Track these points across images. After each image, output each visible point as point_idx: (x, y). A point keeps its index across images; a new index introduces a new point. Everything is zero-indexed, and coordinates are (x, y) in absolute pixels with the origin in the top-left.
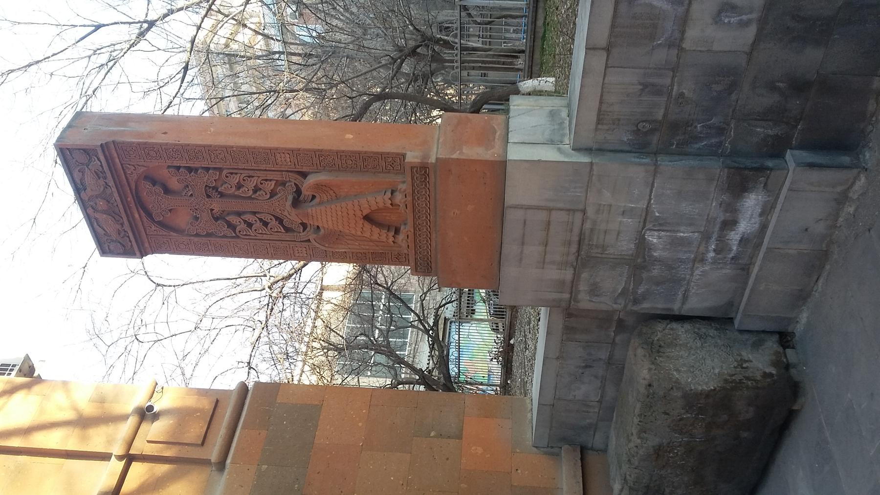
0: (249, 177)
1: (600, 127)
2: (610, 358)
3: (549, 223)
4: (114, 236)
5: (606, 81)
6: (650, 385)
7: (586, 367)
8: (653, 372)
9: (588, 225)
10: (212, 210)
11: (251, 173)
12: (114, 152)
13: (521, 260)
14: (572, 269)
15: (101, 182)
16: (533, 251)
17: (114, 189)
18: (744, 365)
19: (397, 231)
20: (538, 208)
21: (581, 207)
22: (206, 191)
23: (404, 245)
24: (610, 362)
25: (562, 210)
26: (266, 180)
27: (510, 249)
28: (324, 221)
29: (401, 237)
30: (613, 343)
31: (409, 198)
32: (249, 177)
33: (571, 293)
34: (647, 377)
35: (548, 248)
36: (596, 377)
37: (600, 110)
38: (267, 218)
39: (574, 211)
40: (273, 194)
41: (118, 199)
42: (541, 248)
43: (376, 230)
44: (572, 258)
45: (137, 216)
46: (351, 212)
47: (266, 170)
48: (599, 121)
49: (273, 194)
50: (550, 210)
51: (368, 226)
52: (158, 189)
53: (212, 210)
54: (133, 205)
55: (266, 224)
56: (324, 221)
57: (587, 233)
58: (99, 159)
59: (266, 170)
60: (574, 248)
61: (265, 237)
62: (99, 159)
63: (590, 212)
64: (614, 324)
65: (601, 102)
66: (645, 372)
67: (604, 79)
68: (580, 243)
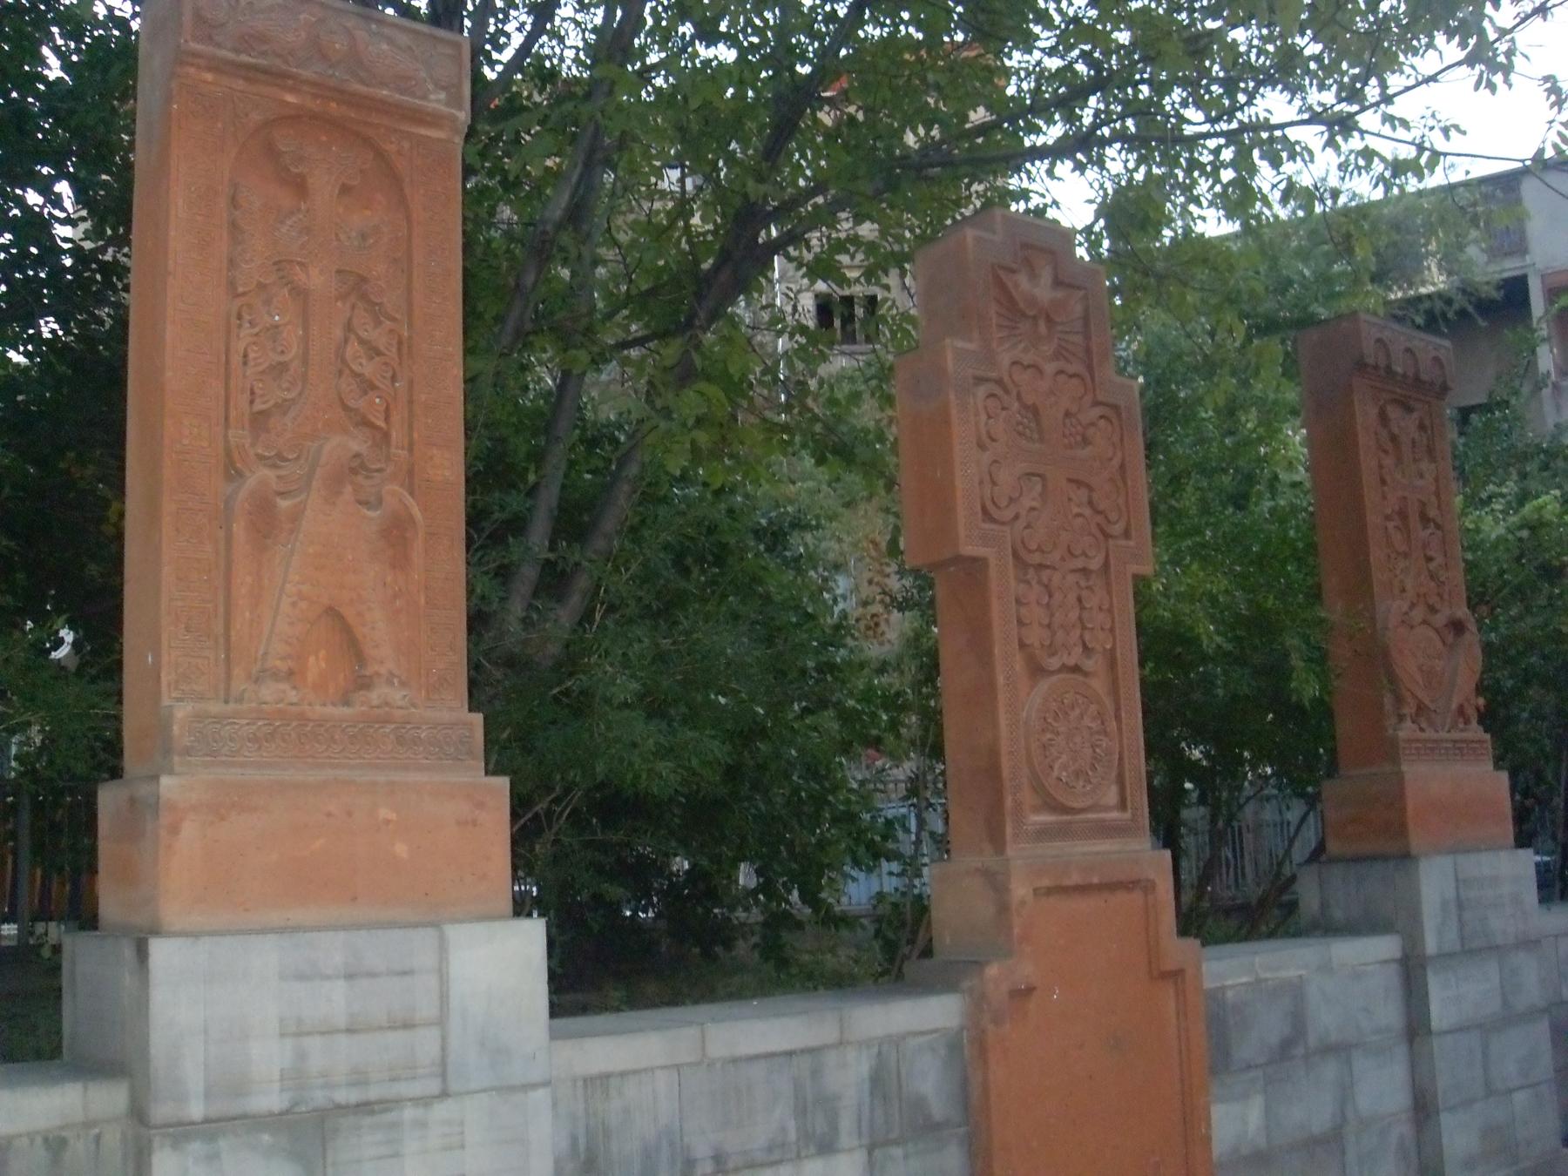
1: (580, 1083)
3: (408, 1025)
13: (301, 977)
14: (285, 1105)
16: (335, 1001)
20: (444, 997)
21: (454, 1086)
25: (443, 1049)
27: (332, 949)
33: (207, 1121)
35: (343, 1040)
39: (444, 1076)
42: (342, 1021)
44: (319, 1098)
48: (588, 1081)
50: (441, 1021)
60: (344, 1096)
63: (441, 1111)
68: (365, 1108)
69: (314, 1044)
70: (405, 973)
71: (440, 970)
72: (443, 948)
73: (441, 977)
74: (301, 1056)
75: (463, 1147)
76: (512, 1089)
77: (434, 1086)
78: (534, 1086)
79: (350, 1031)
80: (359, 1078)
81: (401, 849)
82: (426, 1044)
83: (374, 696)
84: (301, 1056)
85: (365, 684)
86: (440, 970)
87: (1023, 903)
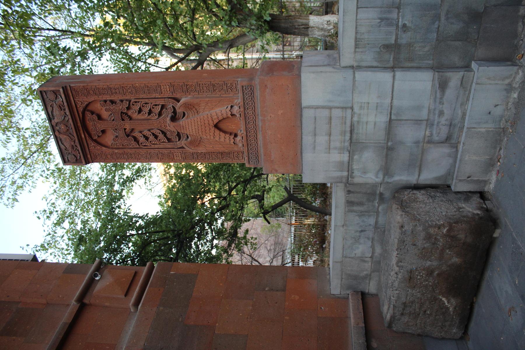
0: (146, 104)
1: (357, 50)
2: (376, 222)
3: (330, 118)
4: (70, 150)
5: (358, 17)
6: (402, 227)
7: (362, 231)
8: (404, 216)
9: (355, 119)
10: (125, 129)
11: (147, 101)
12: (70, 92)
13: (314, 148)
14: (348, 153)
15: (62, 112)
16: (322, 139)
17: (70, 117)
18: (460, 210)
19: (236, 135)
20: (323, 107)
21: (350, 105)
22: (121, 116)
23: (240, 145)
24: (376, 226)
25: (338, 108)
26: (156, 105)
27: (307, 139)
28: (190, 129)
29: (239, 138)
30: (378, 212)
31: (242, 109)
32: (146, 104)
33: (348, 171)
34: (400, 220)
35: (332, 137)
36: (368, 239)
37: (356, 38)
38: (157, 132)
39: (346, 108)
40: (160, 114)
41: (72, 123)
42: (327, 138)
43: (222, 134)
44: (347, 144)
45: (83, 136)
46: (206, 122)
47: (155, 98)
48: (356, 46)
49: (160, 114)
50: (330, 108)
51: (217, 132)
52: (95, 117)
53: (125, 129)
54: (81, 128)
55: (156, 137)
56: (190, 129)
57: (356, 124)
58: (61, 97)
59: (155, 98)
60: (348, 137)
61: (156, 146)
62: (61, 97)
63: (356, 109)
64: (377, 197)
65: (356, 33)
66: (399, 217)
67: (357, 16)
68: (351, 132)
69: (332, 145)
70: (315, 119)
72: (308, 107)
73: (317, 108)
74: (335, 148)
75: (368, 103)
76: (354, 85)
77: (349, 111)
78: (354, 77)
79: (330, 135)
80: (344, 133)
82: (337, 113)
83: (238, 115)
84: (335, 148)
86: (315, 108)
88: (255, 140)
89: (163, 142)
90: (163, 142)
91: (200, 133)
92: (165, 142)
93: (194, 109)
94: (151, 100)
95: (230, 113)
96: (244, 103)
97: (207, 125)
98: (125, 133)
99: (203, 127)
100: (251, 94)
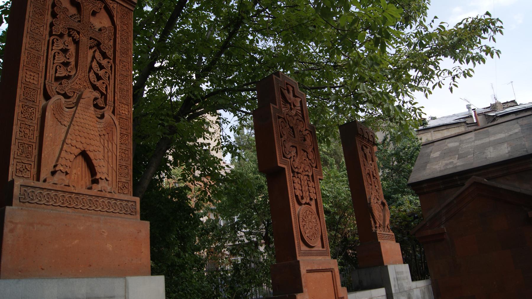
0: (109, 77)
12: (128, 6)
22: (96, 40)
26: (106, 88)
31: (109, 195)
40: (95, 88)
51: (77, 151)
53: (79, 33)
55: (66, 64)
70: (111, 297)
71: (125, 296)
72: (126, 287)
81: (109, 246)
83: (99, 187)
85: (95, 181)
87: (304, 275)
88: (63, 203)
89: (56, 70)
90: (56, 70)
91: (77, 128)
92: (56, 72)
93: (104, 132)
94: (113, 87)
95: (103, 177)
96: (116, 200)
97: (88, 141)
98: (73, 29)
99: (86, 135)
100: (127, 211)
